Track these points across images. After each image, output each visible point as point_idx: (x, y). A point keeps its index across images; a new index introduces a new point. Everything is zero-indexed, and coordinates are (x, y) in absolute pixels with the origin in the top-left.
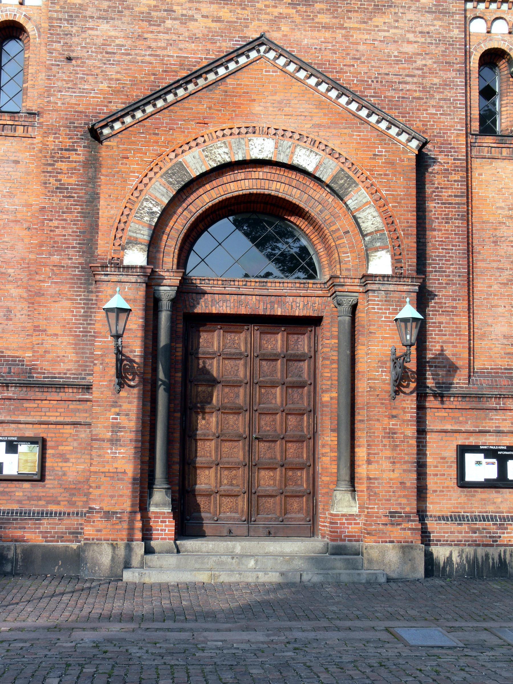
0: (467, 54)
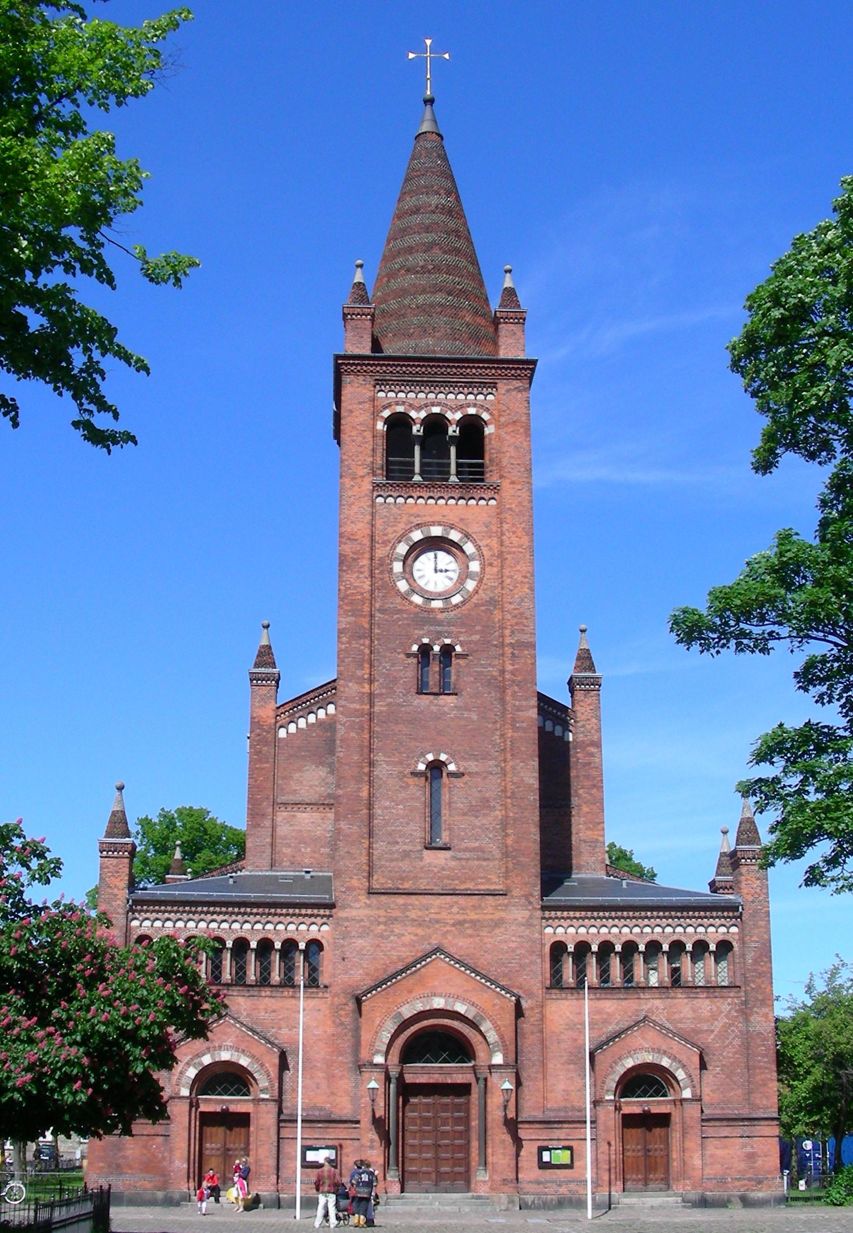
0: (543, 945)
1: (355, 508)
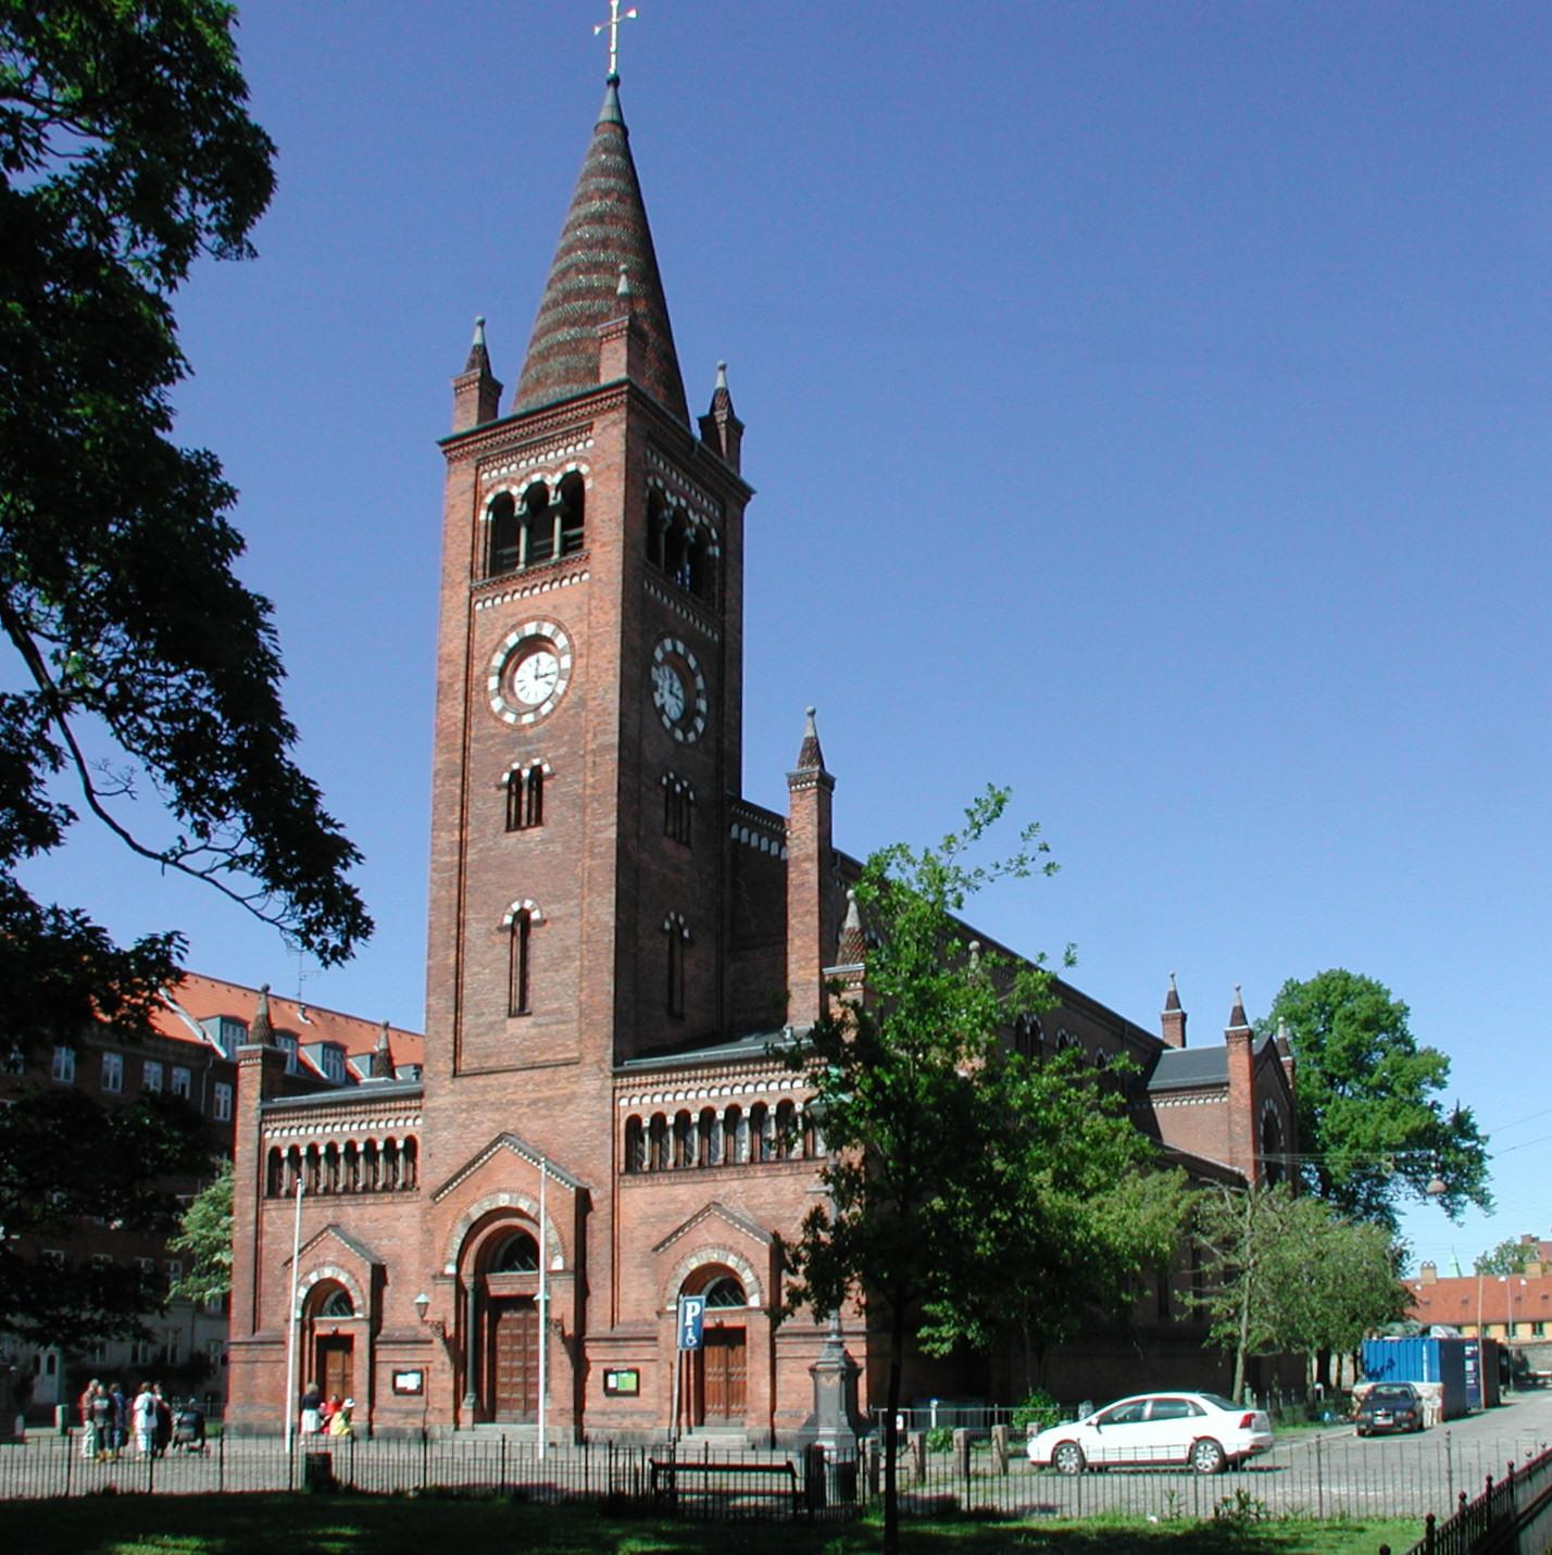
1: (453, 623)
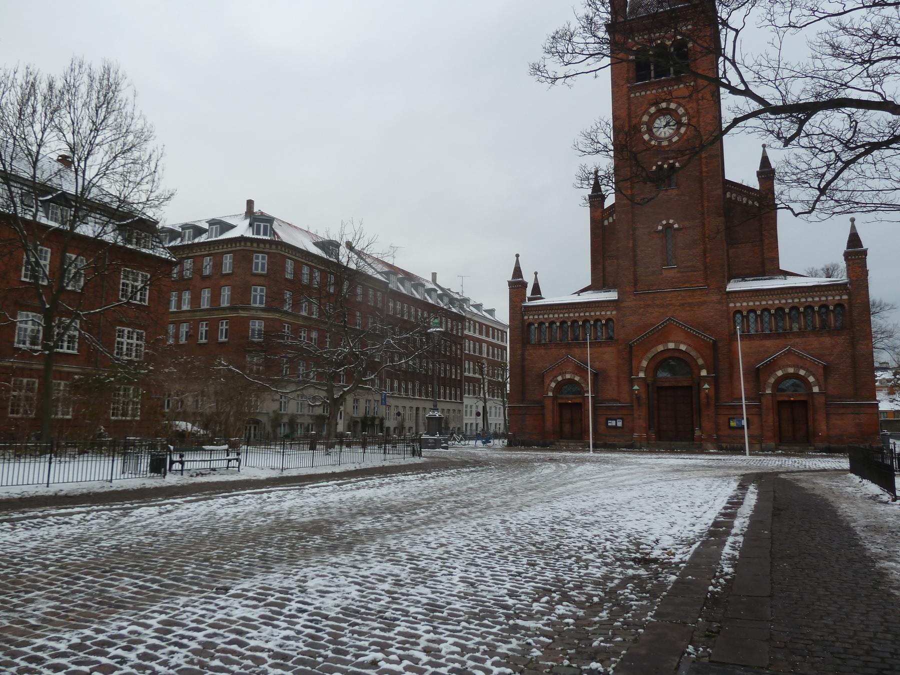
0: (729, 313)
